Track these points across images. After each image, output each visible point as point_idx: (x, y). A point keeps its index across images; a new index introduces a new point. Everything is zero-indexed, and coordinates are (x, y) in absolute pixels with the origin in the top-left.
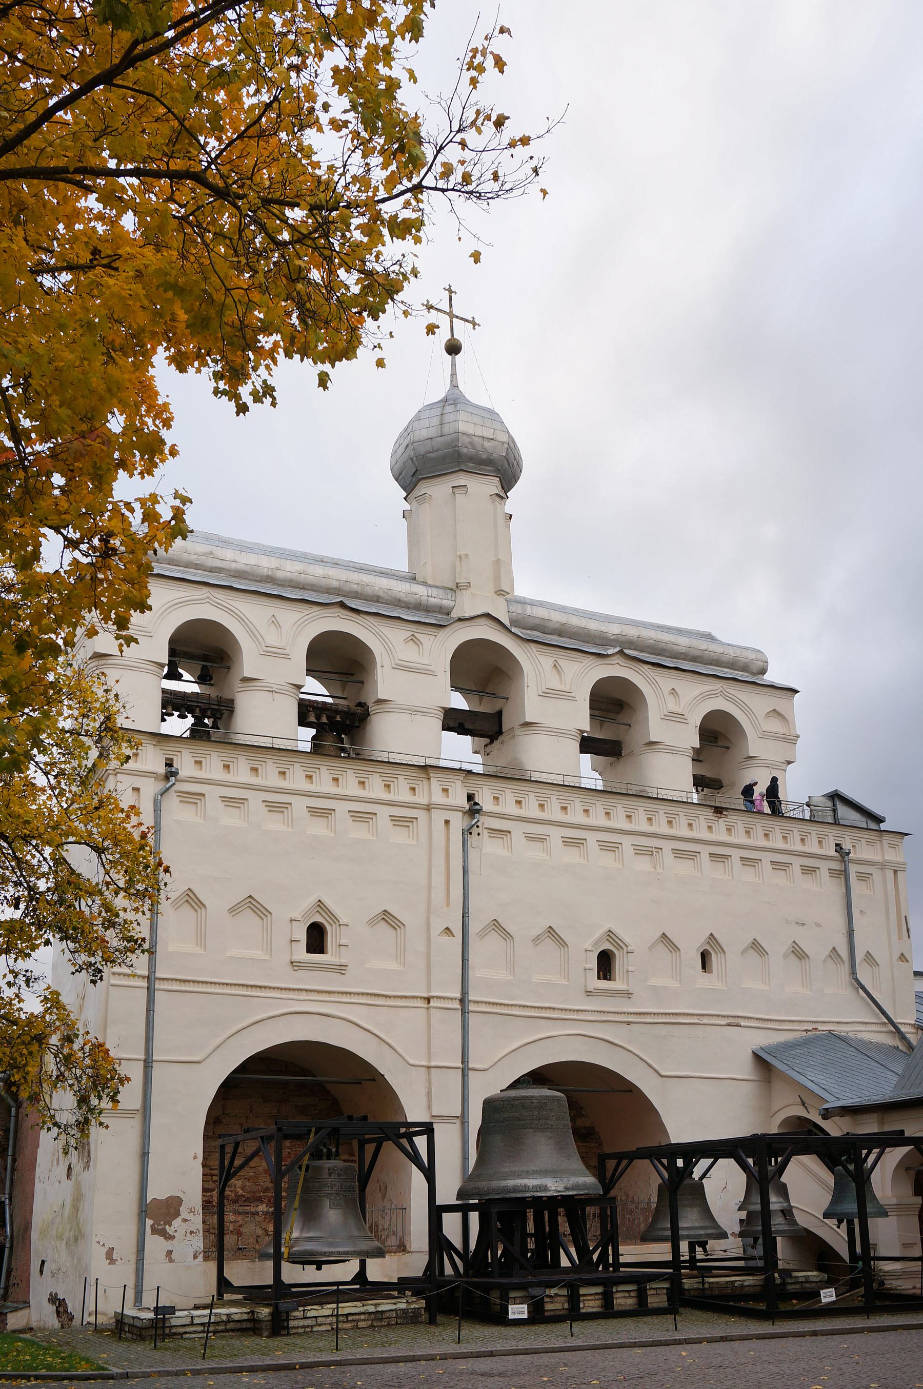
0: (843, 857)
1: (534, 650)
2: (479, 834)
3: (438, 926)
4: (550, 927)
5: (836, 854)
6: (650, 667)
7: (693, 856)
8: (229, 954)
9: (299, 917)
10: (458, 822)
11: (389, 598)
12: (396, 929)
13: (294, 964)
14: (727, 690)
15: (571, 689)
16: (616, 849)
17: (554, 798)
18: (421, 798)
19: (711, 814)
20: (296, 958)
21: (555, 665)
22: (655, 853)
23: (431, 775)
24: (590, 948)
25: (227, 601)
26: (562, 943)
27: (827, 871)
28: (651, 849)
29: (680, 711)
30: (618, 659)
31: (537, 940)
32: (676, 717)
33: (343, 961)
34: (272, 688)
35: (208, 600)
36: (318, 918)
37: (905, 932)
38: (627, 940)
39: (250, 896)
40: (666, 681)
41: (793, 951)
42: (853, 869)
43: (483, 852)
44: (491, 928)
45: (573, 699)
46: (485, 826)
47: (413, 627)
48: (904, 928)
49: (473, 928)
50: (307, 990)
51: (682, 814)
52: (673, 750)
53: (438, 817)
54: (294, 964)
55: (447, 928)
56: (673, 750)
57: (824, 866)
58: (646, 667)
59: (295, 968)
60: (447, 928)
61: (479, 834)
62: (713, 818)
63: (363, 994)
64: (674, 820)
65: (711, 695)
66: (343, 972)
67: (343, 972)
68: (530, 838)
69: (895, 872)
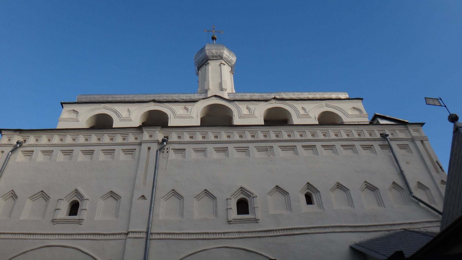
0: (385, 138)
2: (167, 152)
3: (137, 194)
4: (206, 190)
5: (381, 138)
8: (21, 219)
9: (62, 198)
10: (155, 147)
12: (117, 200)
13: (54, 221)
15: (254, 113)
16: (246, 150)
17: (210, 133)
20: (55, 218)
21: (247, 108)
22: (269, 150)
23: (143, 130)
24: (229, 197)
25: (111, 107)
26: (213, 197)
27: (379, 147)
30: (274, 101)
31: (198, 197)
33: (81, 218)
36: (76, 198)
37: (440, 170)
38: (252, 190)
39: (42, 191)
40: (299, 105)
41: (366, 187)
42: (394, 144)
43: (169, 159)
44: (172, 195)
45: (256, 117)
47: (184, 104)
48: (438, 167)
49: (159, 194)
50: (58, 234)
53: (145, 147)
54: (54, 221)
55: (143, 196)
59: (55, 223)
60: (143, 196)
61: (167, 152)
63: (90, 234)
64: (279, 134)
65: (322, 107)
66: (80, 223)
67: (80, 223)
68: (196, 150)
69: (422, 141)
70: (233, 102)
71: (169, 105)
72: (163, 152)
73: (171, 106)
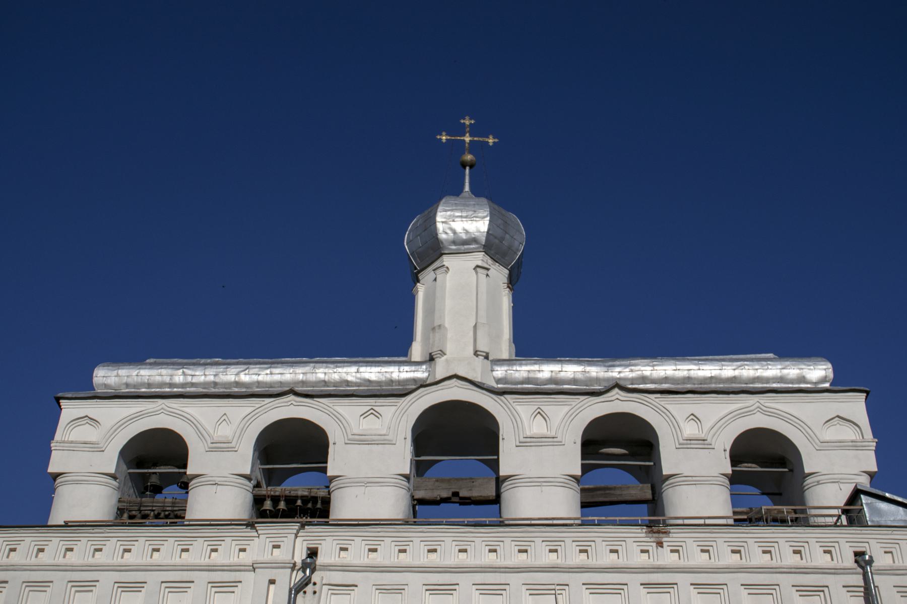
1: (511, 402)
2: (315, 592)
6: (659, 395)
7: (618, 588)
11: (358, 381)
14: (766, 405)
17: (417, 541)
18: (245, 559)
19: (644, 535)
25: (179, 408)
28: (553, 587)
29: (702, 436)
32: (702, 443)
34: (215, 481)
35: (162, 411)
40: (679, 407)
46: (324, 582)
51: (598, 540)
52: (694, 481)
56: (694, 481)
57: (835, 582)
58: (652, 396)
61: (315, 592)
62: (648, 539)
68: (383, 589)
70: (502, 398)
71: (331, 405)
72: (305, 592)
73: (337, 408)
